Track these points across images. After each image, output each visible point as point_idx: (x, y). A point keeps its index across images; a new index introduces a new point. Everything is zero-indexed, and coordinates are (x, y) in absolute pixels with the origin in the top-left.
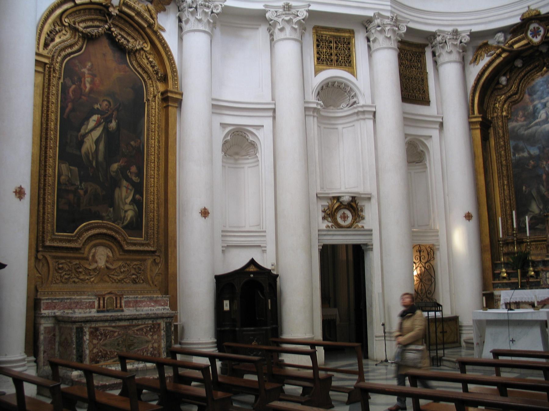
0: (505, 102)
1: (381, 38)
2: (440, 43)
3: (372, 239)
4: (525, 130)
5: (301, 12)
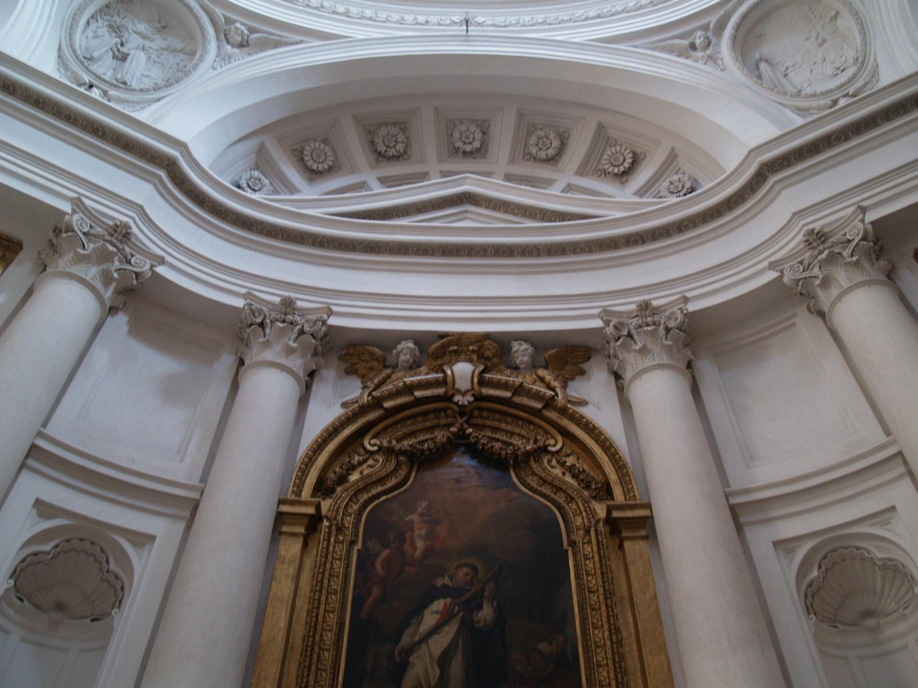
5: (850, 230)
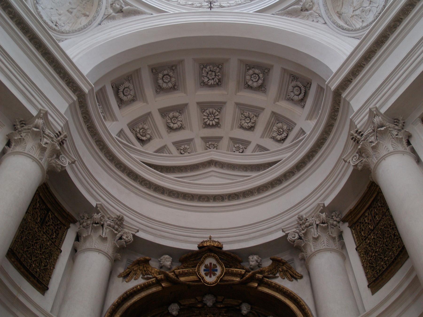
2: (96, 223)
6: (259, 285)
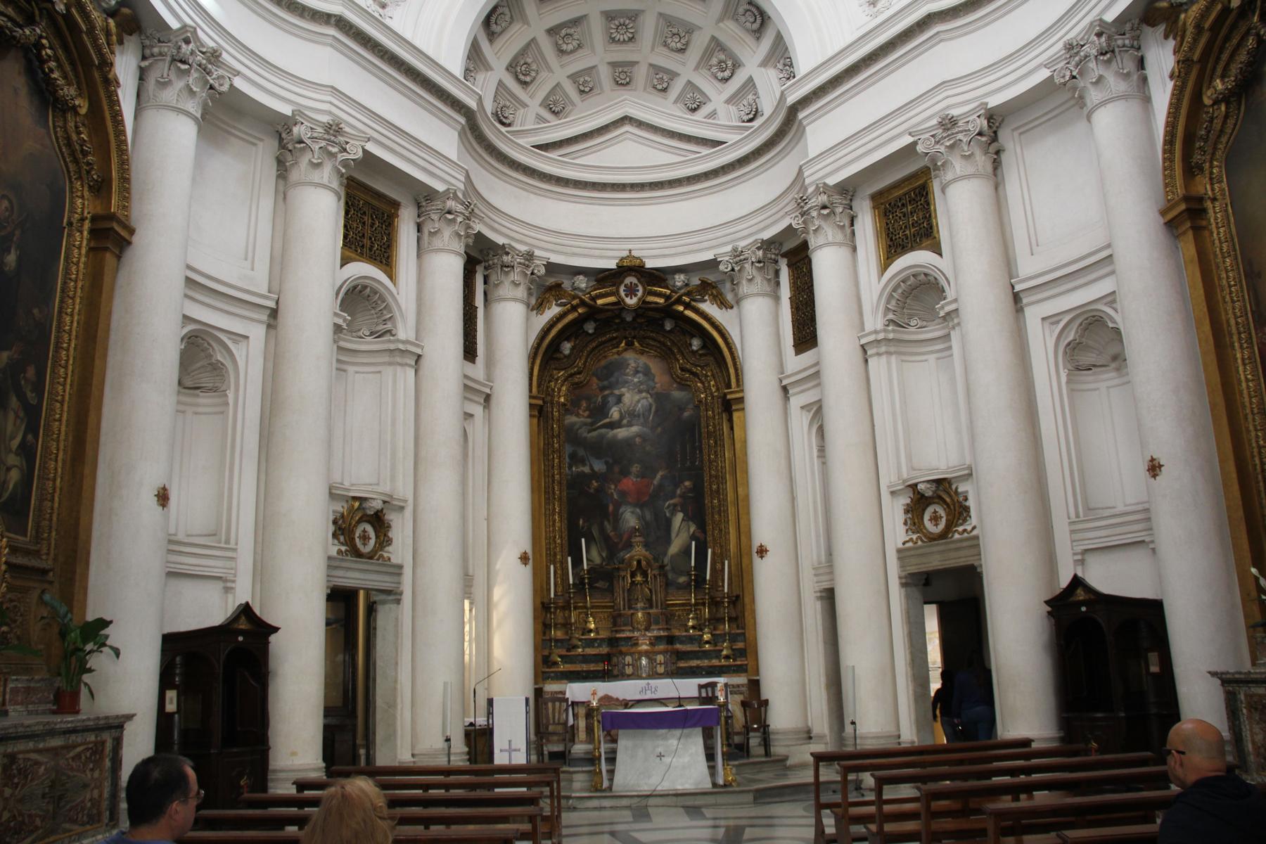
0: (565, 380)
1: (447, 232)
2: (506, 266)
3: (399, 583)
4: (588, 433)
6: (685, 308)
